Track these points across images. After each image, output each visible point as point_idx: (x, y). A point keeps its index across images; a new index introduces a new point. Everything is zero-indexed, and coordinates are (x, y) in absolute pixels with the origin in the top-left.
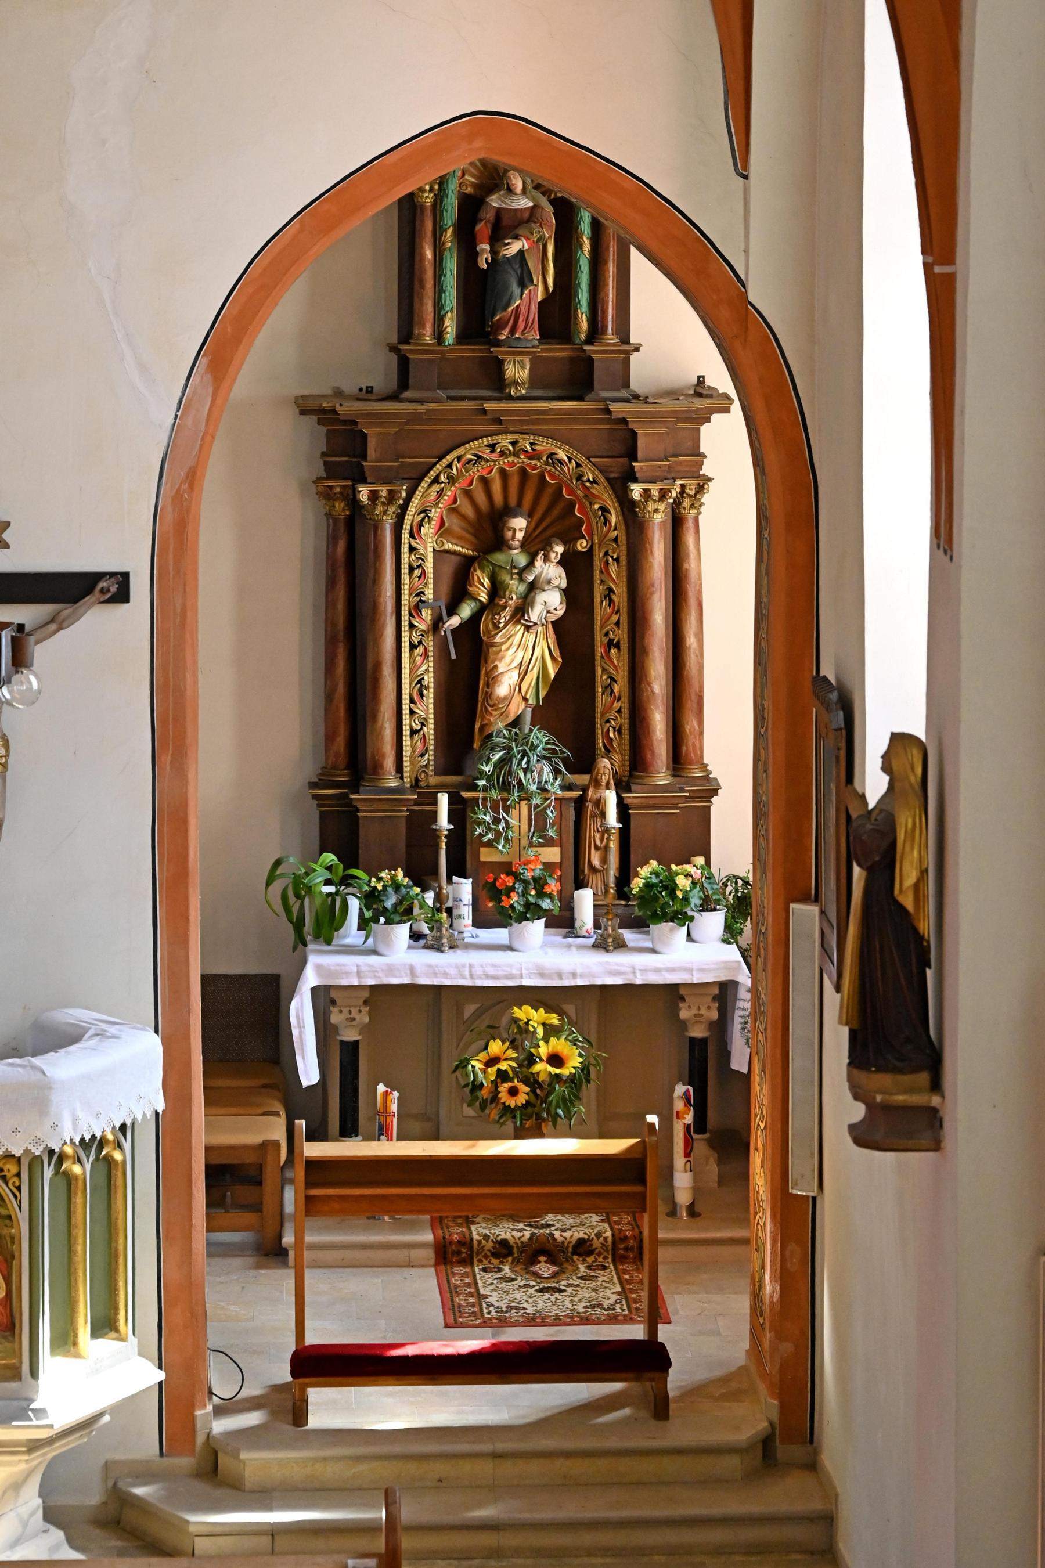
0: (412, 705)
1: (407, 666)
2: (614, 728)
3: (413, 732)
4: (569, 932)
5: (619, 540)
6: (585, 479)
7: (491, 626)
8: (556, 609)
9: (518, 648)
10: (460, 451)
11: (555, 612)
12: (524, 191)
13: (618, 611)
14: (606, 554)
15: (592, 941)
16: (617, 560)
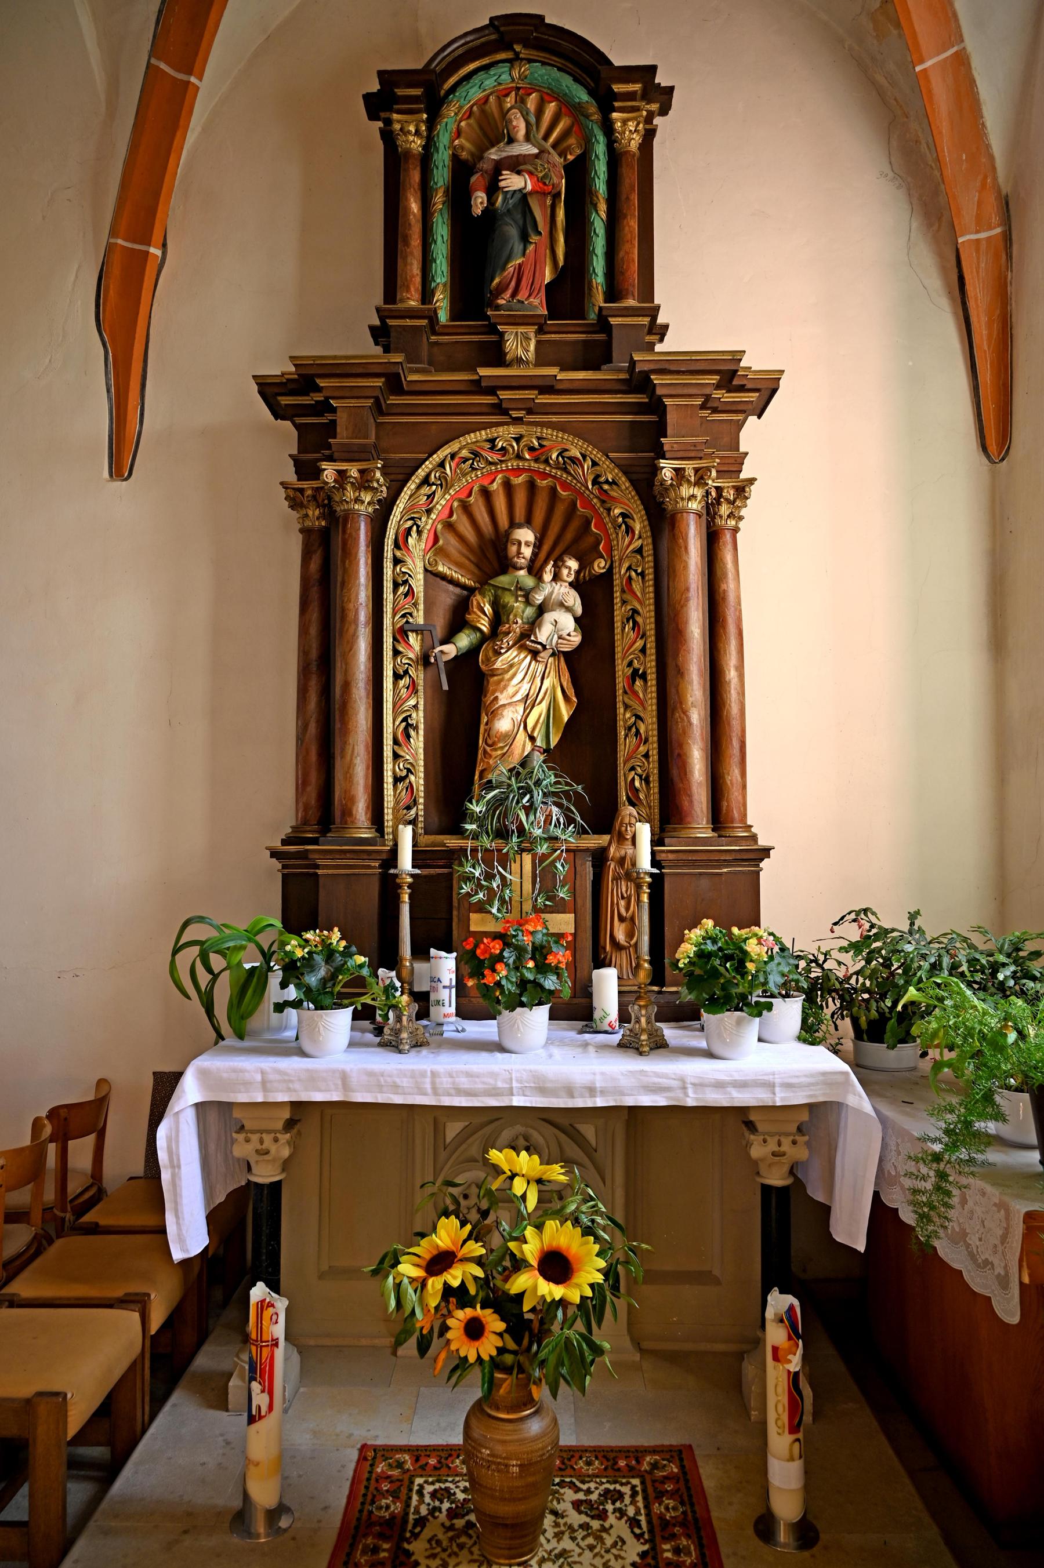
0: (396, 747)
1: (390, 699)
2: (640, 776)
3: (397, 780)
4: (586, 1025)
5: (645, 548)
6: (602, 479)
7: (491, 654)
8: (569, 635)
9: (524, 678)
10: (454, 446)
11: (568, 637)
12: (528, 138)
13: (644, 636)
14: (629, 568)
15: (616, 1038)
16: (642, 575)
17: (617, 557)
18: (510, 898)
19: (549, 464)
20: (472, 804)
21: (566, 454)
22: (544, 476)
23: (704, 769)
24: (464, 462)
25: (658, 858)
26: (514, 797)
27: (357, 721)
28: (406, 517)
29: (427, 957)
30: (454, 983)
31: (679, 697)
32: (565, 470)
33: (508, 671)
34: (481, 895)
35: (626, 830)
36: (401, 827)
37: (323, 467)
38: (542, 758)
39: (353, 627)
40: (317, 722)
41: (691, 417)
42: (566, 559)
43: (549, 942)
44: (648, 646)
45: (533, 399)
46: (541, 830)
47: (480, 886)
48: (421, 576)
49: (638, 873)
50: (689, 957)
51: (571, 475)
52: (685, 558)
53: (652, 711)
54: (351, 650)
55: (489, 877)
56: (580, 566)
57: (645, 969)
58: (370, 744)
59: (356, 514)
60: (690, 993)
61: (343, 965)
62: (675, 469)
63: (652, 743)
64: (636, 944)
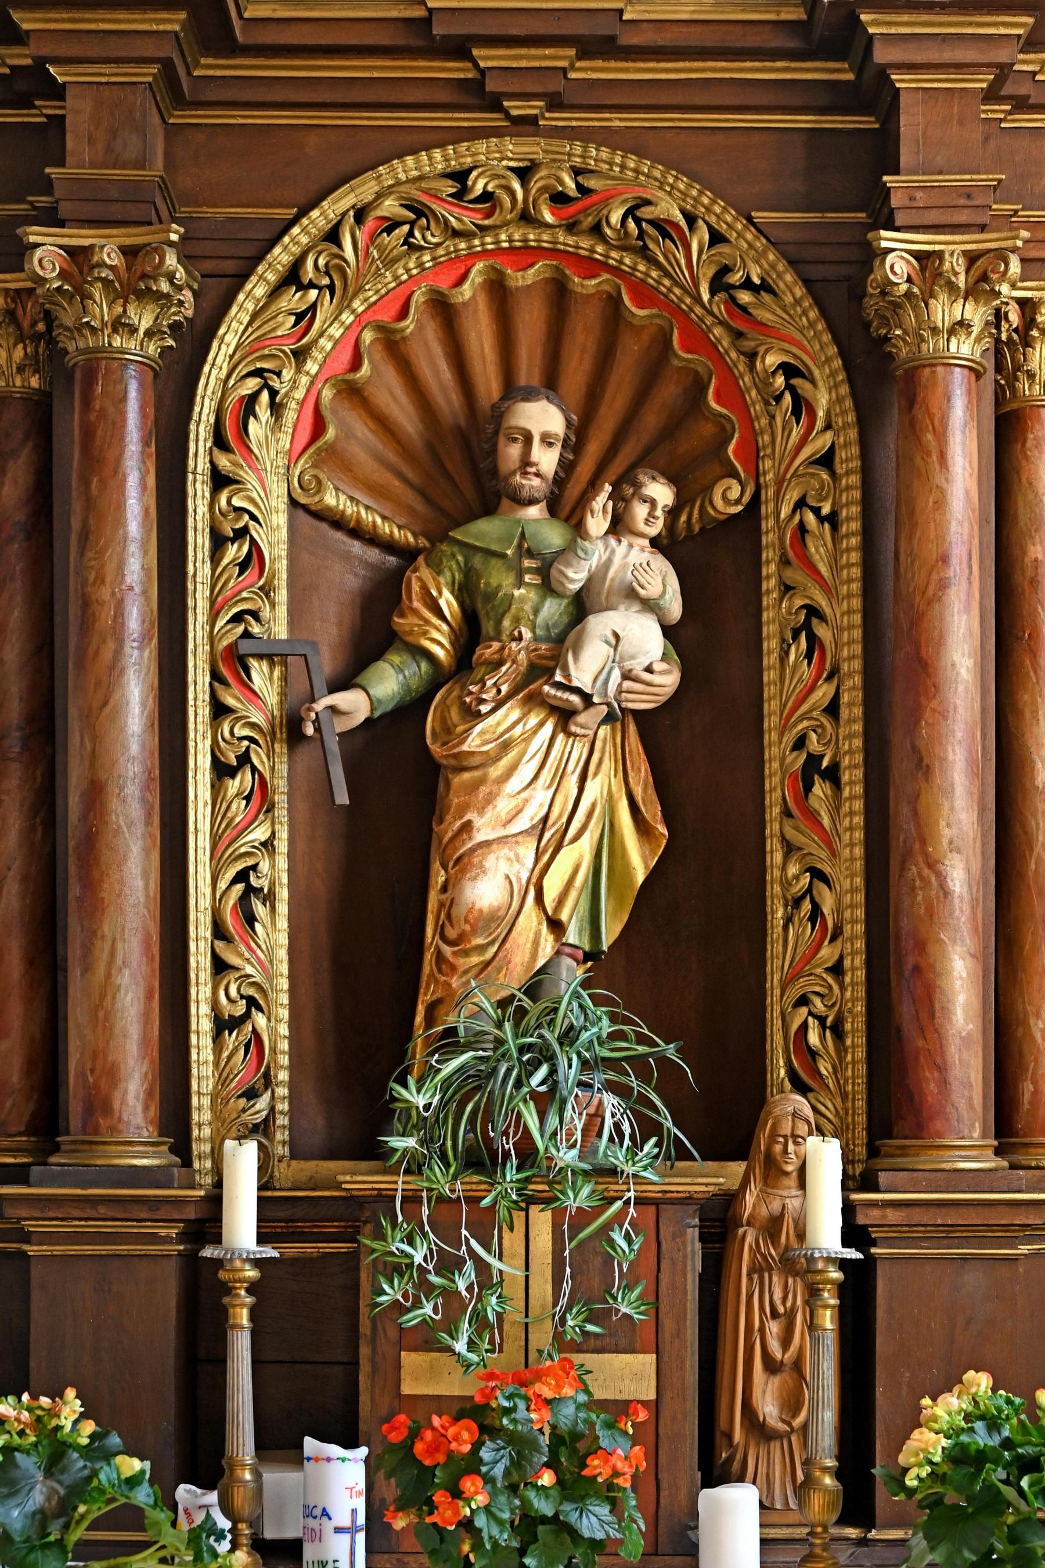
0: (219, 945)
1: (205, 826)
2: (822, 1020)
3: (223, 1025)
5: (841, 454)
6: (736, 278)
7: (455, 715)
8: (649, 670)
9: (536, 777)
10: (364, 190)
11: (647, 676)
14: (801, 504)
16: (833, 520)
17: (770, 476)
18: (499, 1316)
19: (603, 239)
20: (405, 1086)
21: (645, 212)
22: (591, 266)
23: (976, 1004)
24: (389, 230)
25: (861, 1220)
26: (509, 1071)
27: (122, 881)
28: (243, 369)
29: (297, 1459)
30: (361, 1520)
31: (918, 826)
32: (643, 252)
33: (497, 759)
34: (428, 1309)
35: (785, 1151)
36: (229, 1144)
37: (32, 239)
38: (580, 973)
39: (111, 645)
40: (25, 879)
41: (961, 123)
42: (643, 478)
43: (591, 1425)
44: (845, 698)
45: (564, 70)
46: (575, 1152)
47: (426, 1288)
48: (281, 519)
49: (811, 1260)
50: (931, 1463)
51: (659, 266)
52: (938, 479)
53: (852, 859)
54: (105, 703)
55: (449, 1265)
56: (678, 495)
57: (826, 1490)
58: (155, 938)
59: (119, 360)
60: (932, 1549)
61: (89, 1479)
62: (918, 256)
63: (852, 939)
64: (805, 1426)
